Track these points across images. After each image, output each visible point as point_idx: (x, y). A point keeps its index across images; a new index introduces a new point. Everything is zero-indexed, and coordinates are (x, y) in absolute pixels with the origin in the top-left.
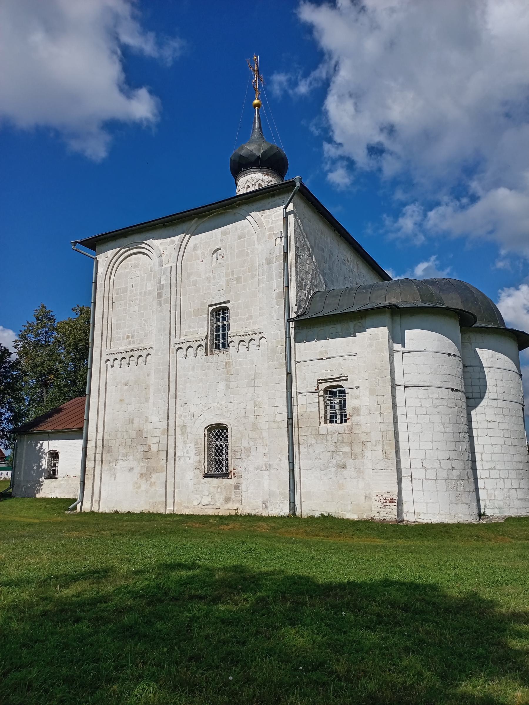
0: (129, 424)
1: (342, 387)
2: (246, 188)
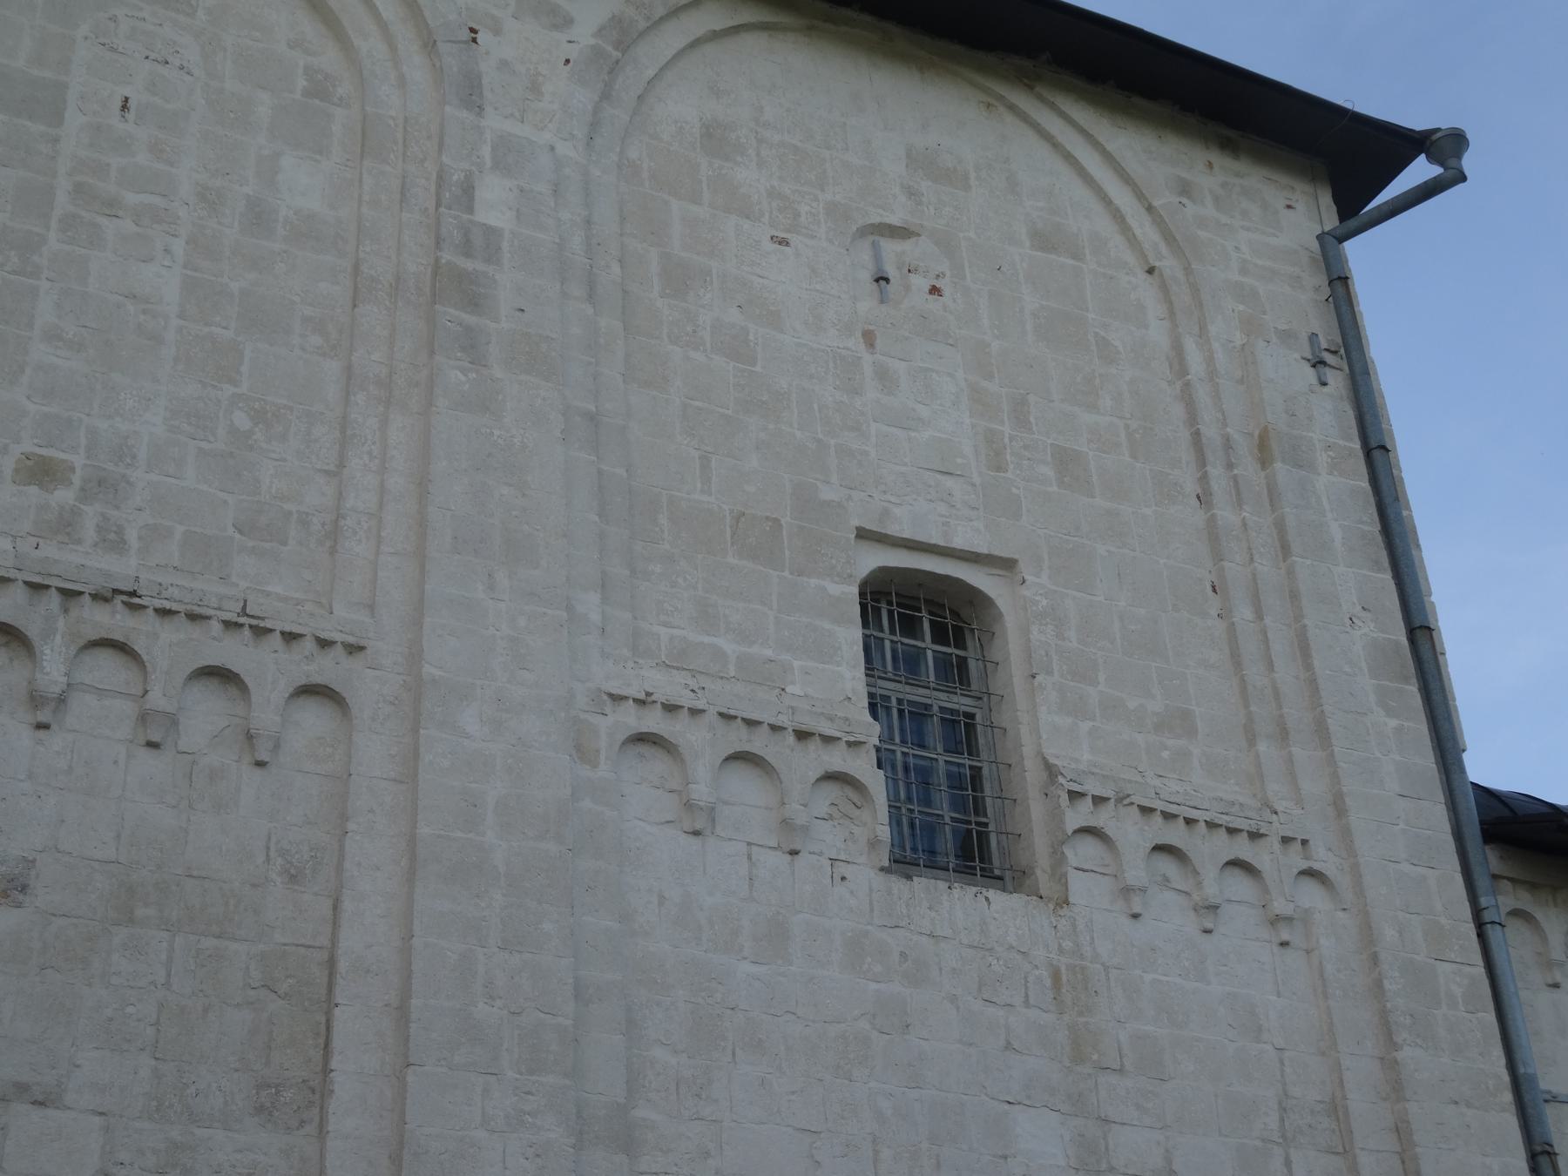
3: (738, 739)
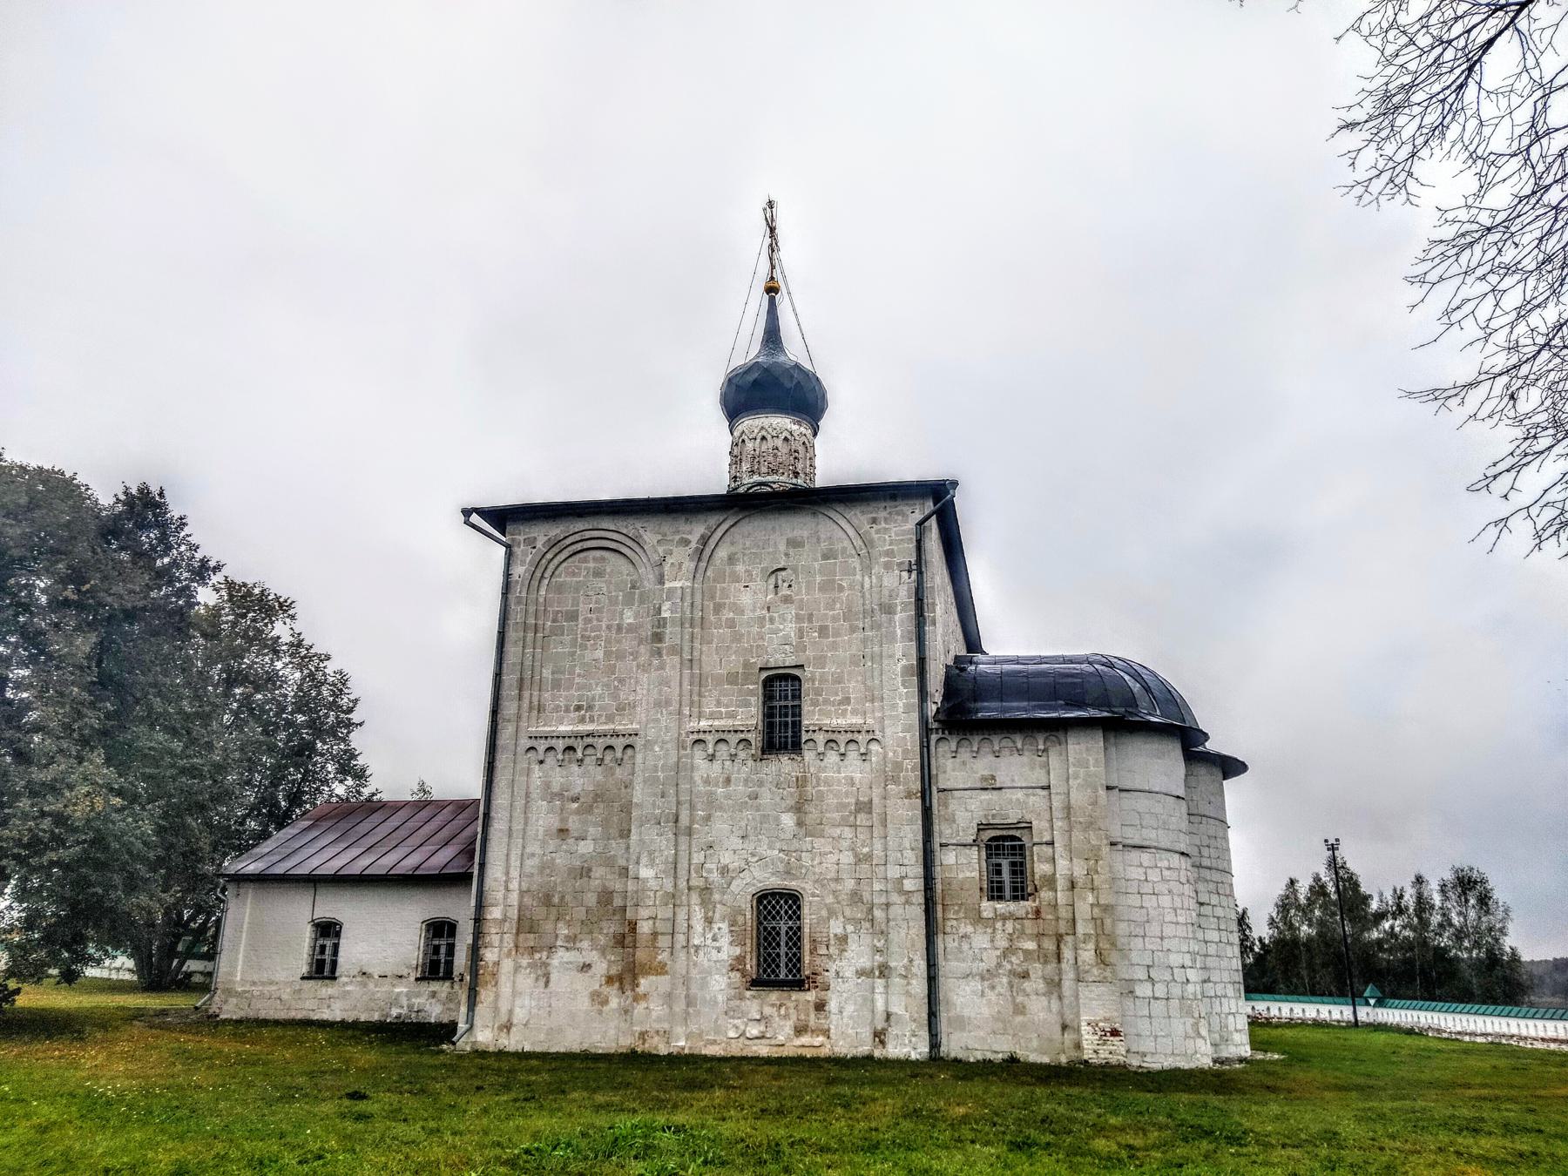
1: (1020, 840)
2: (758, 440)
3: (718, 736)
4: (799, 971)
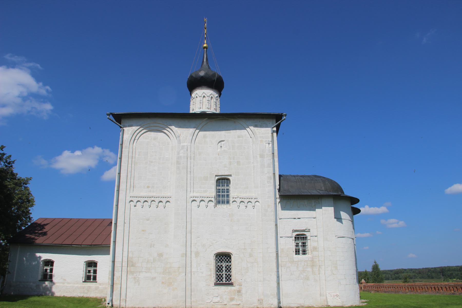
0: (151, 247)
2: (202, 97)
3: (201, 199)
4: (231, 280)
